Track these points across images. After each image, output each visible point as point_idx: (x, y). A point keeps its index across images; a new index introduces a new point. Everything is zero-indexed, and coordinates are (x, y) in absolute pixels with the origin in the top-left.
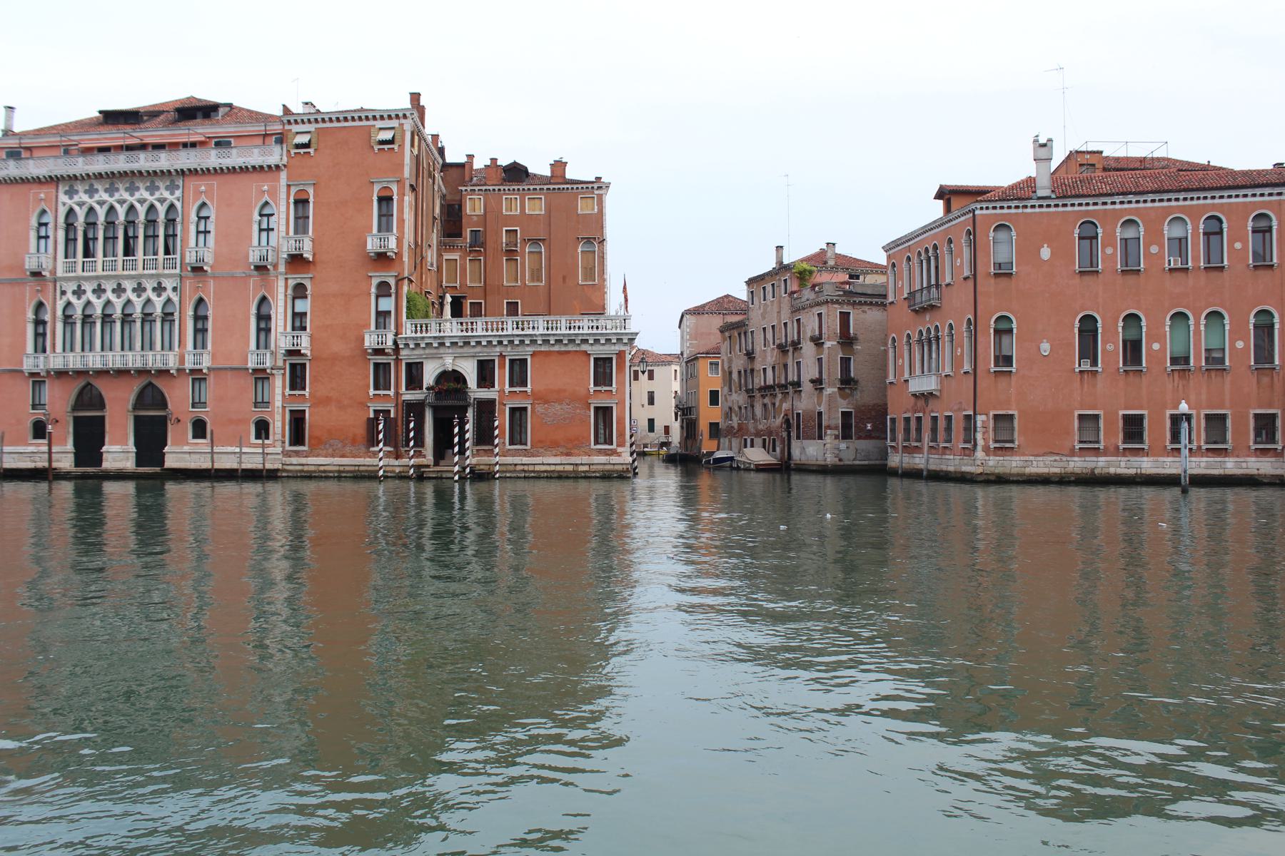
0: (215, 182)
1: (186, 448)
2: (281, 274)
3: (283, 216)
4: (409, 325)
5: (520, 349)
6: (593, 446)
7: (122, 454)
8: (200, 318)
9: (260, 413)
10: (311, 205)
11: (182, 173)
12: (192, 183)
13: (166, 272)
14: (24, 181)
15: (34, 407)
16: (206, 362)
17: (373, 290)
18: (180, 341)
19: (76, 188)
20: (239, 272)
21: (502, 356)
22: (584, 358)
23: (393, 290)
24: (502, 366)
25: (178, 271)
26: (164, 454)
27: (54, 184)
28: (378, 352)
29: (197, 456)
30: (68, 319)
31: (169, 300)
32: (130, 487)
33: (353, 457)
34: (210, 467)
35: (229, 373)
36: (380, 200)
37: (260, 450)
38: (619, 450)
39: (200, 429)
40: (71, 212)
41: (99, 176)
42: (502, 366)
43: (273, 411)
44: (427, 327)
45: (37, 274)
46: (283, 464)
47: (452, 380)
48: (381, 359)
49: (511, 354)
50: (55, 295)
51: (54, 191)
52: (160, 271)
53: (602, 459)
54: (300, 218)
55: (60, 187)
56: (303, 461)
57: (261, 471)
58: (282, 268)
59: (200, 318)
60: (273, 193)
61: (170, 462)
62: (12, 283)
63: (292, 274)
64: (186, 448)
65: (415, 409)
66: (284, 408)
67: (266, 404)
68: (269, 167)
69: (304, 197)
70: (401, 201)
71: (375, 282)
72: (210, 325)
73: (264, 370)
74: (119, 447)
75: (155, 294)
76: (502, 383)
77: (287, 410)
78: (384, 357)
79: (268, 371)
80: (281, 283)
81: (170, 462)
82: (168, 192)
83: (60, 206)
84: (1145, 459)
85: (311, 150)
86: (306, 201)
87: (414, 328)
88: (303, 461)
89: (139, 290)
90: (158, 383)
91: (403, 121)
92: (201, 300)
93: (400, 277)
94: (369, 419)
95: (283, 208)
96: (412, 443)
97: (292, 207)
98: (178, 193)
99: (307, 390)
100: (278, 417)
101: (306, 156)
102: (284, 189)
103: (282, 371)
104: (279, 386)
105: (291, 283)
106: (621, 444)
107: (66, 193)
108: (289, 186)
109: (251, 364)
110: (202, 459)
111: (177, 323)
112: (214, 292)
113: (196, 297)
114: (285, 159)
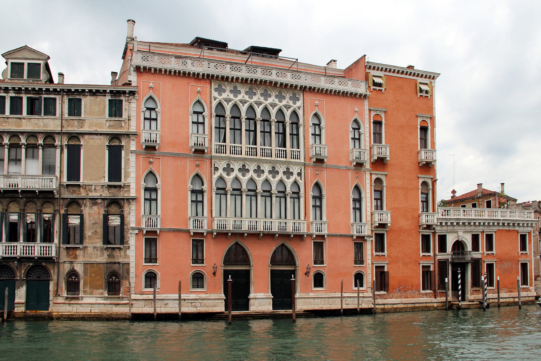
1: (311, 295)
3: (367, 130)
7: (265, 300)
10: (383, 126)
11: (304, 89)
12: (310, 98)
13: (293, 160)
14: (185, 75)
17: (420, 186)
18: (305, 214)
22: (516, 233)
23: (431, 187)
25: (302, 160)
27: (208, 81)
28: (429, 227)
29: (319, 300)
30: (222, 191)
32: (267, 324)
34: (340, 308)
35: (339, 240)
37: (356, 295)
39: (319, 280)
40: (220, 104)
41: (245, 81)
47: (459, 245)
48: (427, 232)
52: (289, 159)
55: (213, 85)
57: (340, 310)
58: (368, 166)
60: (361, 114)
61: (301, 305)
63: (374, 171)
64: (311, 295)
65: (443, 264)
67: (362, 262)
68: (361, 95)
69: (379, 119)
71: (421, 181)
72: (352, 205)
74: (263, 294)
76: (483, 249)
77: (374, 266)
78: (429, 231)
79: (366, 238)
80: (368, 176)
81: (301, 305)
85: (383, 89)
90: (290, 245)
93: (434, 180)
95: (367, 125)
97: (372, 124)
98: (299, 103)
99: (386, 252)
100: (369, 271)
101: (379, 92)
102: (367, 112)
103: (371, 239)
104: (369, 248)
105: (374, 177)
107: (216, 90)
108: (370, 110)
110: (322, 302)
111: (302, 200)
112: (327, 180)
114: (368, 92)
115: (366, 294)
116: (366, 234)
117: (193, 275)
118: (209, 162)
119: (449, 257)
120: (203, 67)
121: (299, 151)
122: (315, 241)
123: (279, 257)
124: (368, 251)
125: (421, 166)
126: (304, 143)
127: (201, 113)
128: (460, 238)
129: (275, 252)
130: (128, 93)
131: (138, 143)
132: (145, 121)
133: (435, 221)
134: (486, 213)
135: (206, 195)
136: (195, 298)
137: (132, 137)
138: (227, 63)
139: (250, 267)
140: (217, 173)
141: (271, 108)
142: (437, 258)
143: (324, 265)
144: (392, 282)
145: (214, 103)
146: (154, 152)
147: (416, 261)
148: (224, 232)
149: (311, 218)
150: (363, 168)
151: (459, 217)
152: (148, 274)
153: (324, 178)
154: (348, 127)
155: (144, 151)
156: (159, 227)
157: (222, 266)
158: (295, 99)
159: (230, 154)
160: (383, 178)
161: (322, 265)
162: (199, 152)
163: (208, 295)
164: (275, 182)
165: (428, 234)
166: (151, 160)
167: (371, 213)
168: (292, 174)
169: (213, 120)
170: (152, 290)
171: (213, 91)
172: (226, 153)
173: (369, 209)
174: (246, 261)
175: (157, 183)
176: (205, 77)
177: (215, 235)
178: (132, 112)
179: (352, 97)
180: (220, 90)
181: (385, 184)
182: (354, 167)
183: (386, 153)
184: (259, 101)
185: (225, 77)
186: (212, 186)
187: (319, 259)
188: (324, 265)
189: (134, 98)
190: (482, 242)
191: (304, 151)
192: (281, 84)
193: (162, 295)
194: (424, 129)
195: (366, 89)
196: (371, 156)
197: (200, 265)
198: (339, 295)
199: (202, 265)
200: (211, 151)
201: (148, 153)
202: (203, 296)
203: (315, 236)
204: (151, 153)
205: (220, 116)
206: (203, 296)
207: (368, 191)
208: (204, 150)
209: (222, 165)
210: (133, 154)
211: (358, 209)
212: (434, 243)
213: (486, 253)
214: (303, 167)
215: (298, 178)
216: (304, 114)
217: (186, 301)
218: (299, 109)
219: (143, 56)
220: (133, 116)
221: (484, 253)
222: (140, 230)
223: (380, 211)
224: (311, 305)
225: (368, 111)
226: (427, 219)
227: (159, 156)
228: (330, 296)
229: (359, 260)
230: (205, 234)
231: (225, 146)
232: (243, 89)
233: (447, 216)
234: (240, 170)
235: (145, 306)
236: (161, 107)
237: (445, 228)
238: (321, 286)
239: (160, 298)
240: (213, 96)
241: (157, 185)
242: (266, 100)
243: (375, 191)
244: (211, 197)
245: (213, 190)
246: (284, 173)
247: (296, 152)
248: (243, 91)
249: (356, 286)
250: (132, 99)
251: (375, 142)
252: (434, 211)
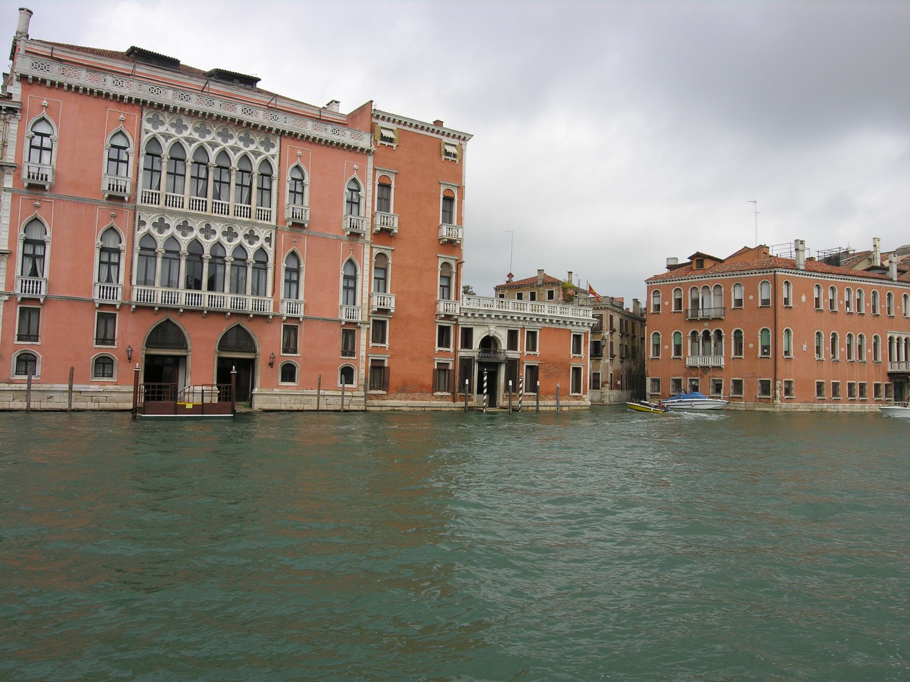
0: (310, 150)
1: (276, 391)
2: (367, 242)
3: (370, 194)
5: (534, 324)
6: (571, 394)
8: (293, 272)
9: (347, 361)
11: (281, 133)
12: (288, 144)
13: (259, 221)
15: (101, 340)
18: (274, 290)
19: (161, 118)
20: (331, 234)
21: (523, 328)
23: (454, 270)
24: (522, 335)
25: (273, 222)
26: (252, 395)
27: (137, 108)
28: (448, 317)
29: (288, 398)
30: (148, 251)
31: (262, 250)
33: (421, 400)
36: (445, 198)
38: (584, 396)
39: (289, 373)
40: (154, 140)
41: (193, 114)
42: (522, 335)
43: (358, 360)
45: (116, 198)
47: (489, 343)
48: (445, 323)
49: (530, 327)
50: (134, 224)
51: (137, 115)
52: (253, 219)
53: (575, 402)
55: (144, 114)
58: (368, 238)
59: (293, 272)
60: (362, 172)
62: (79, 202)
64: (276, 391)
65: (466, 364)
66: (367, 357)
67: (352, 354)
68: (362, 150)
69: (387, 182)
71: (441, 262)
73: (356, 324)
75: (247, 241)
76: (522, 348)
78: (449, 322)
79: (359, 325)
80: (367, 250)
81: (259, 403)
83: (143, 131)
84: (840, 404)
85: (394, 145)
86: (389, 187)
89: (230, 234)
91: (463, 142)
92: (293, 254)
94: (434, 369)
95: (370, 188)
96: (485, 391)
97: (377, 187)
98: (274, 151)
99: (387, 343)
100: (362, 365)
101: (388, 147)
102: (371, 171)
103: (368, 326)
105: (376, 251)
107: (149, 120)
108: (375, 170)
109: (343, 317)
110: (292, 401)
111: (270, 272)
113: (291, 250)
114: (373, 146)
115: (355, 393)
116: (360, 319)
117: (96, 360)
118: (132, 213)
119: (476, 355)
120: (131, 88)
121: (270, 211)
122: (285, 324)
123: (231, 342)
124: (362, 341)
125: (442, 244)
126: (278, 201)
127: (125, 148)
128: (492, 333)
129: (226, 333)
130: (5, 110)
131: (18, 177)
132: (32, 149)
133: (458, 311)
134: (529, 307)
135: (123, 255)
136: (98, 390)
137: (7, 170)
138: (169, 88)
140: (142, 229)
141: (232, 153)
142: (459, 355)
143: (298, 355)
144: (394, 380)
145: (145, 138)
146: (43, 192)
147: (429, 357)
148: (151, 305)
149: (282, 296)
150: (360, 240)
151: (492, 309)
152: (23, 356)
153: (304, 247)
154: (343, 187)
155: (26, 191)
156: (43, 293)
157: (143, 350)
158: (268, 145)
159: (166, 205)
160: (389, 254)
162: (116, 198)
163: (117, 387)
164: (232, 247)
165: (447, 325)
166: (38, 203)
167: (369, 295)
168: (257, 238)
169: (142, 160)
170: (25, 377)
171: (145, 123)
172: (158, 204)
173: (366, 290)
174: (182, 343)
175: (46, 234)
176: (133, 102)
177: (133, 309)
178: (9, 135)
179: (350, 151)
180: (156, 123)
181: (390, 261)
182: (347, 238)
183: (394, 224)
184: (214, 143)
185: (164, 105)
186: (133, 245)
187: (290, 346)
189: (14, 117)
190: (522, 340)
191: (277, 211)
192: (249, 124)
193: (44, 385)
194: (449, 200)
195: (371, 142)
196: (373, 226)
197: (109, 347)
198: (315, 392)
199: (112, 347)
200: (135, 200)
201: (33, 194)
202: (110, 387)
203: (285, 318)
204: (37, 194)
205: (153, 155)
206: (110, 387)
207: (367, 267)
208: (124, 197)
209: (150, 219)
210: (7, 193)
212: (455, 337)
213: (526, 353)
214: (274, 232)
215: (266, 245)
216: (279, 165)
217: (82, 394)
218: (273, 158)
219: (34, 62)
220: (11, 141)
221: (523, 353)
222: (12, 296)
223: (381, 294)
224: (276, 403)
226: (446, 307)
227: (51, 199)
228: (303, 394)
229: (349, 349)
230: (118, 307)
231: (159, 194)
232: (190, 124)
234: (178, 227)
235: (13, 400)
236: (60, 134)
237: (472, 320)
238: (292, 379)
239: (40, 389)
240: (143, 127)
241: (45, 237)
242: (226, 142)
243: (375, 268)
244: (132, 259)
245: (135, 250)
246: (246, 236)
247: (265, 212)
248: (190, 126)
250: (12, 119)
251: (380, 209)
252: (457, 298)
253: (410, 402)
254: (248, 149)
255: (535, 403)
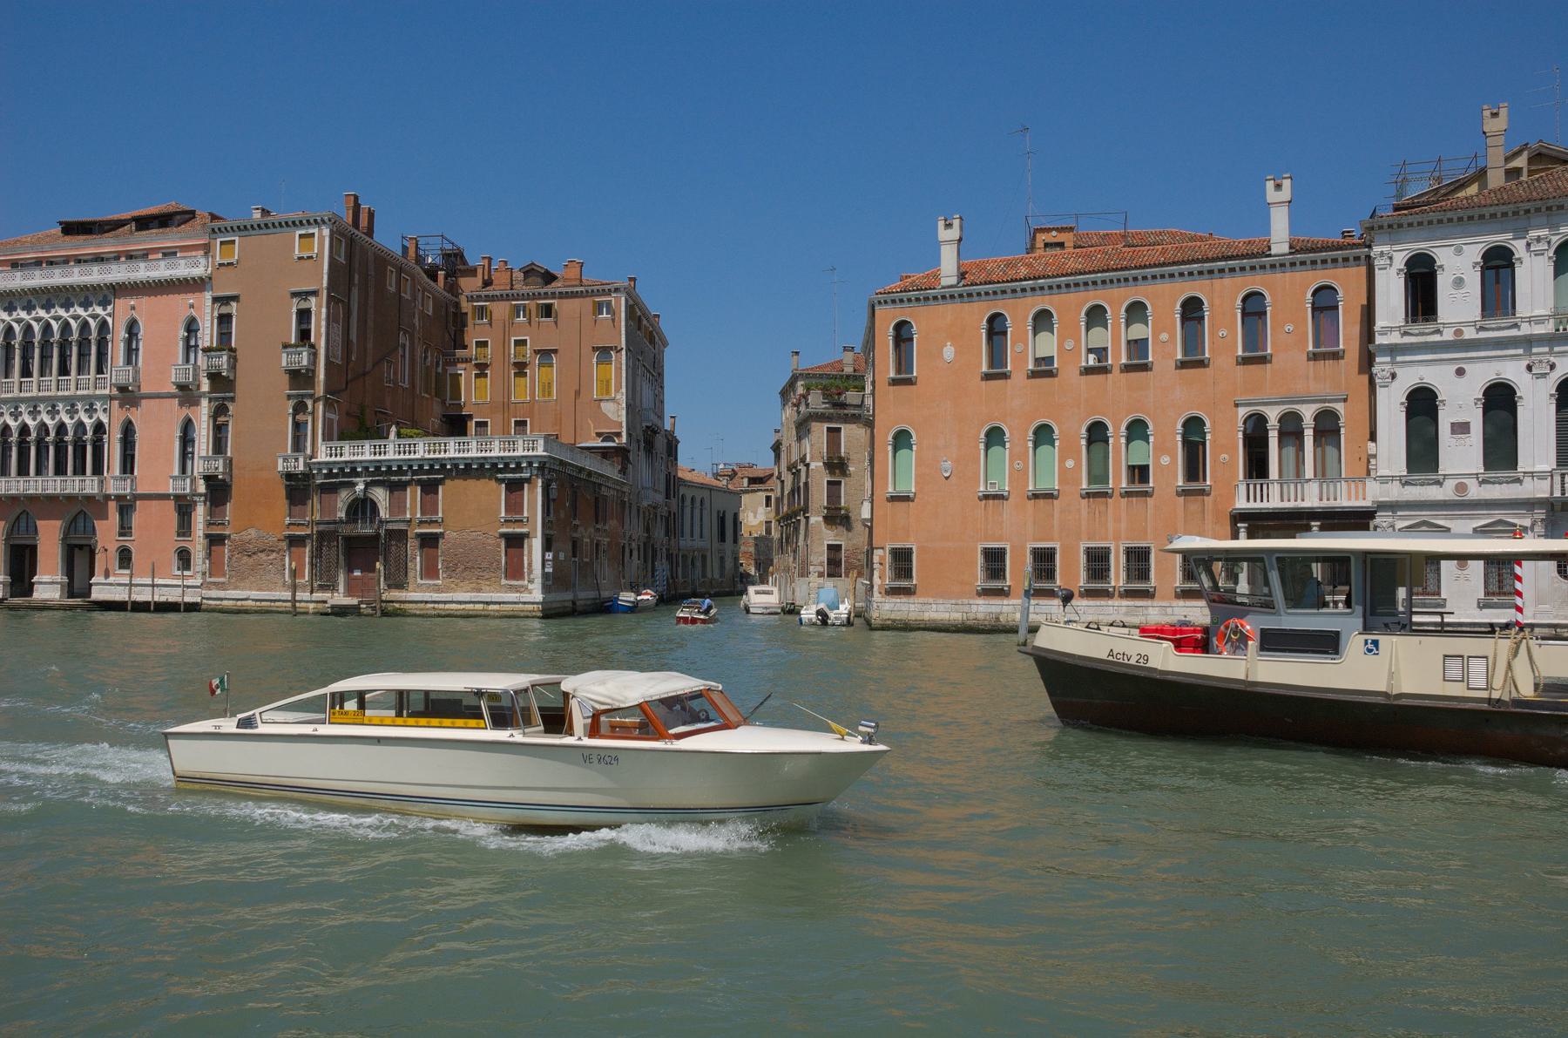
4: (324, 448)
10: (234, 320)
16: (125, 489)
38: (530, 587)
44: (341, 450)
46: (203, 598)
54: (224, 334)
56: (221, 594)
61: (98, 594)
70: (319, 313)
76: (413, 513)
82: (64, 310)
87: (329, 452)
88: (221, 594)
95: (208, 324)
98: (110, 308)
106: (531, 581)
139: (36, 541)
161: (129, 538)
188: (131, 538)
211: (186, 455)
225: (210, 301)
233: (443, 453)
249: (179, 569)
253: (255, 594)
254: (88, 313)
255: (287, 595)
